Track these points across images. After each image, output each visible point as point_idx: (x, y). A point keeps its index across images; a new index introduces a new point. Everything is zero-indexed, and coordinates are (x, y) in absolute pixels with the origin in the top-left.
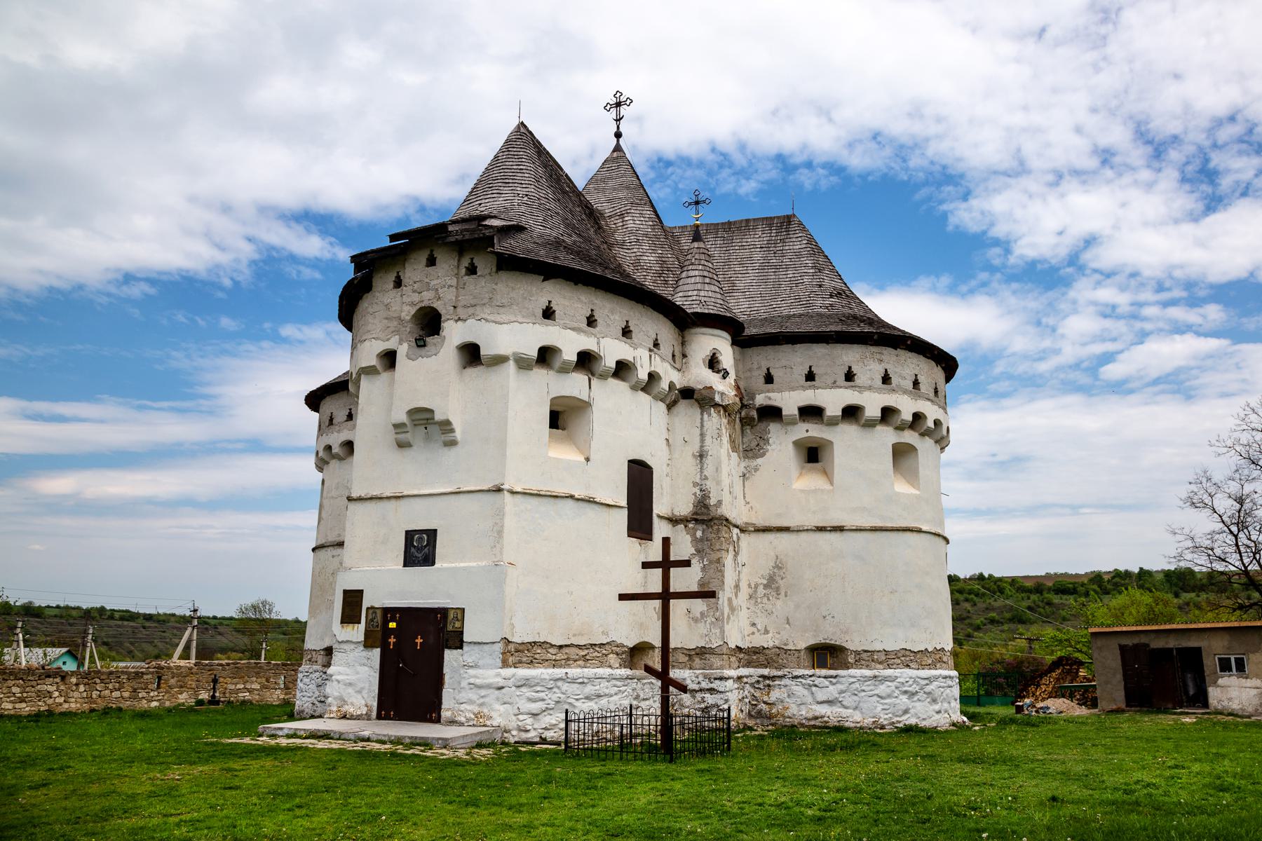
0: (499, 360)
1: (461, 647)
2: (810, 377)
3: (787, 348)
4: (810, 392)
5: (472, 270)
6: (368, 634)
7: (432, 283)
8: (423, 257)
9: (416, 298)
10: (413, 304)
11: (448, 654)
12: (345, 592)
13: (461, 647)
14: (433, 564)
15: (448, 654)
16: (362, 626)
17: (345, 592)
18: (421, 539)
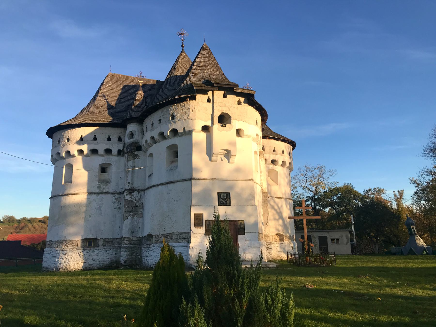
0: (248, 137)
1: (244, 234)
2: (274, 151)
3: (268, 140)
4: (275, 155)
5: (239, 103)
6: (207, 230)
7: (227, 104)
8: (222, 93)
9: (220, 109)
10: (219, 110)
11: (240, 237)
12: (195, 214)
13: (244, 234)
14: (230, 205)
15: (240, 237)
16: (204, 228)
17: (195, 214)
18: (224, 196)
